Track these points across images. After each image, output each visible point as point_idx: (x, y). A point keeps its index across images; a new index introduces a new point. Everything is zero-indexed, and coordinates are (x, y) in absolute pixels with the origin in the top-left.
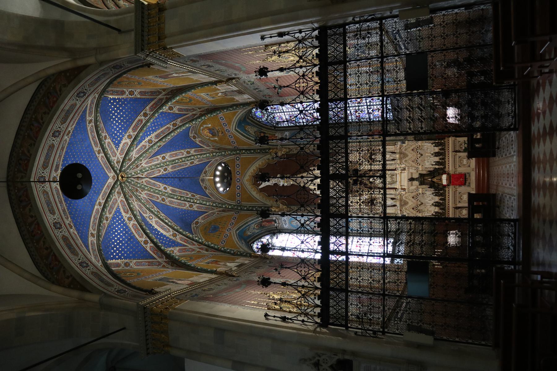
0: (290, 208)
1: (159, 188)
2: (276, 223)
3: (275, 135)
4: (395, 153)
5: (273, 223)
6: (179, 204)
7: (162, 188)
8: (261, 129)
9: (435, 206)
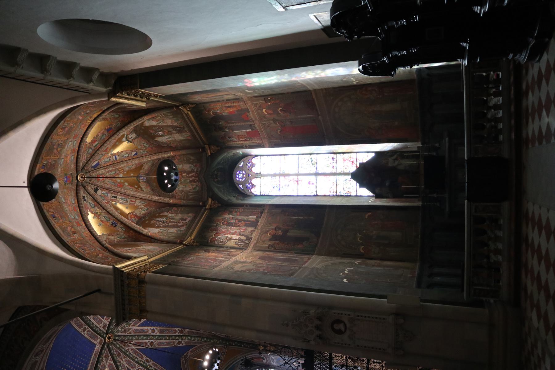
1: (147, 332)
2: (264, 359)
5: (261, 360)
6: (168, 344)
7: (150, 333)
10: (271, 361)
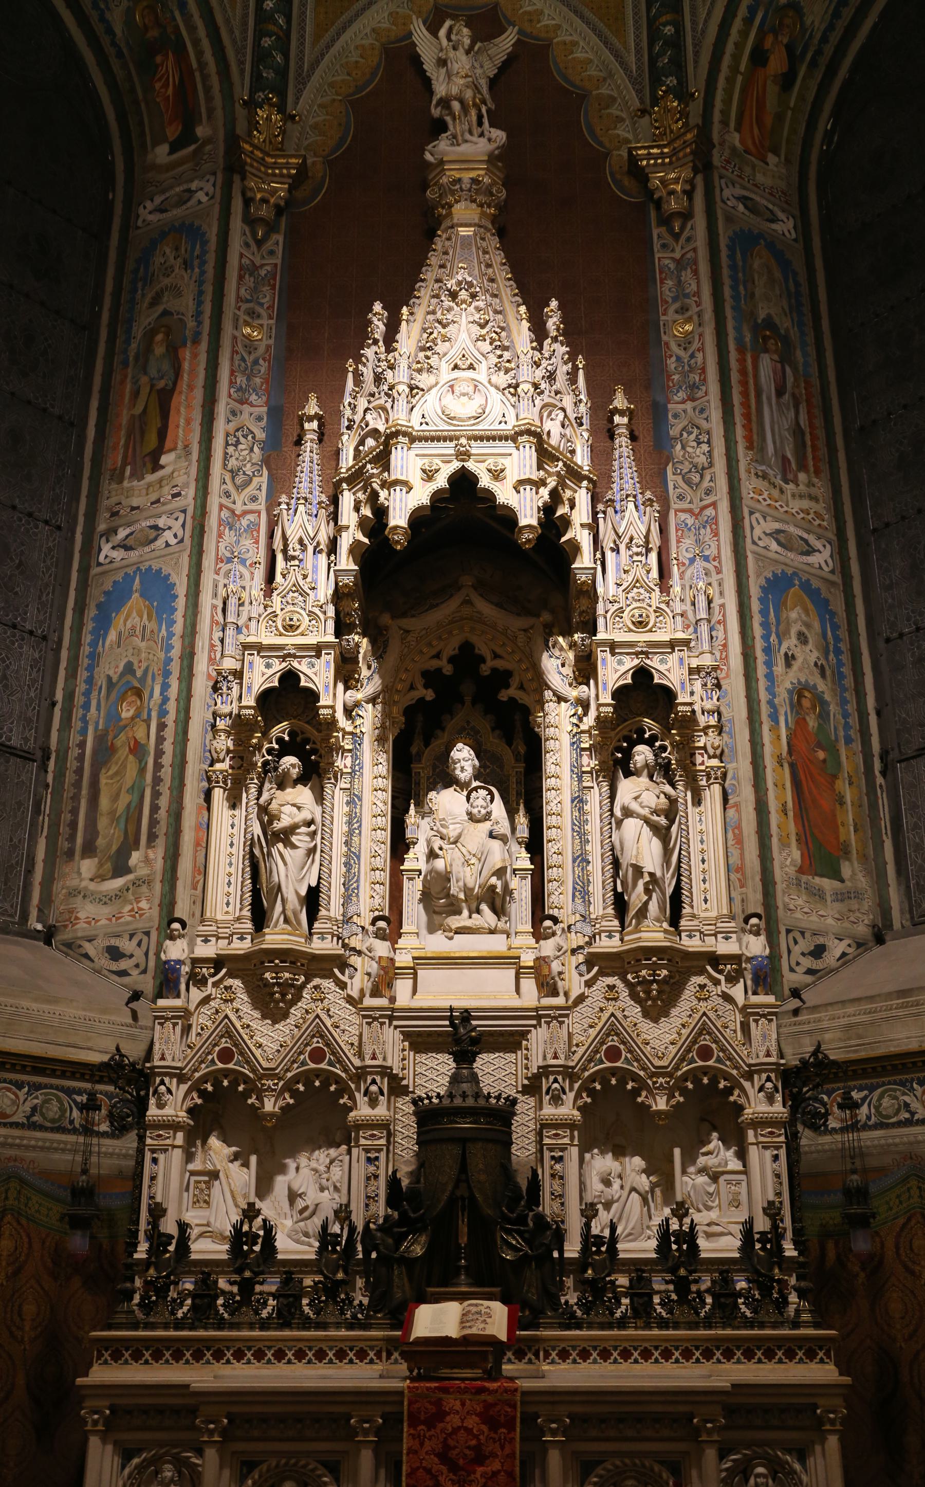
0: (272, 228)
2: (175, 147)
3: (776, 152)
4: (675, 919)
5: (173, 131)
8: (813, 64)
9: (239, 1238)
10: (163, 192)
